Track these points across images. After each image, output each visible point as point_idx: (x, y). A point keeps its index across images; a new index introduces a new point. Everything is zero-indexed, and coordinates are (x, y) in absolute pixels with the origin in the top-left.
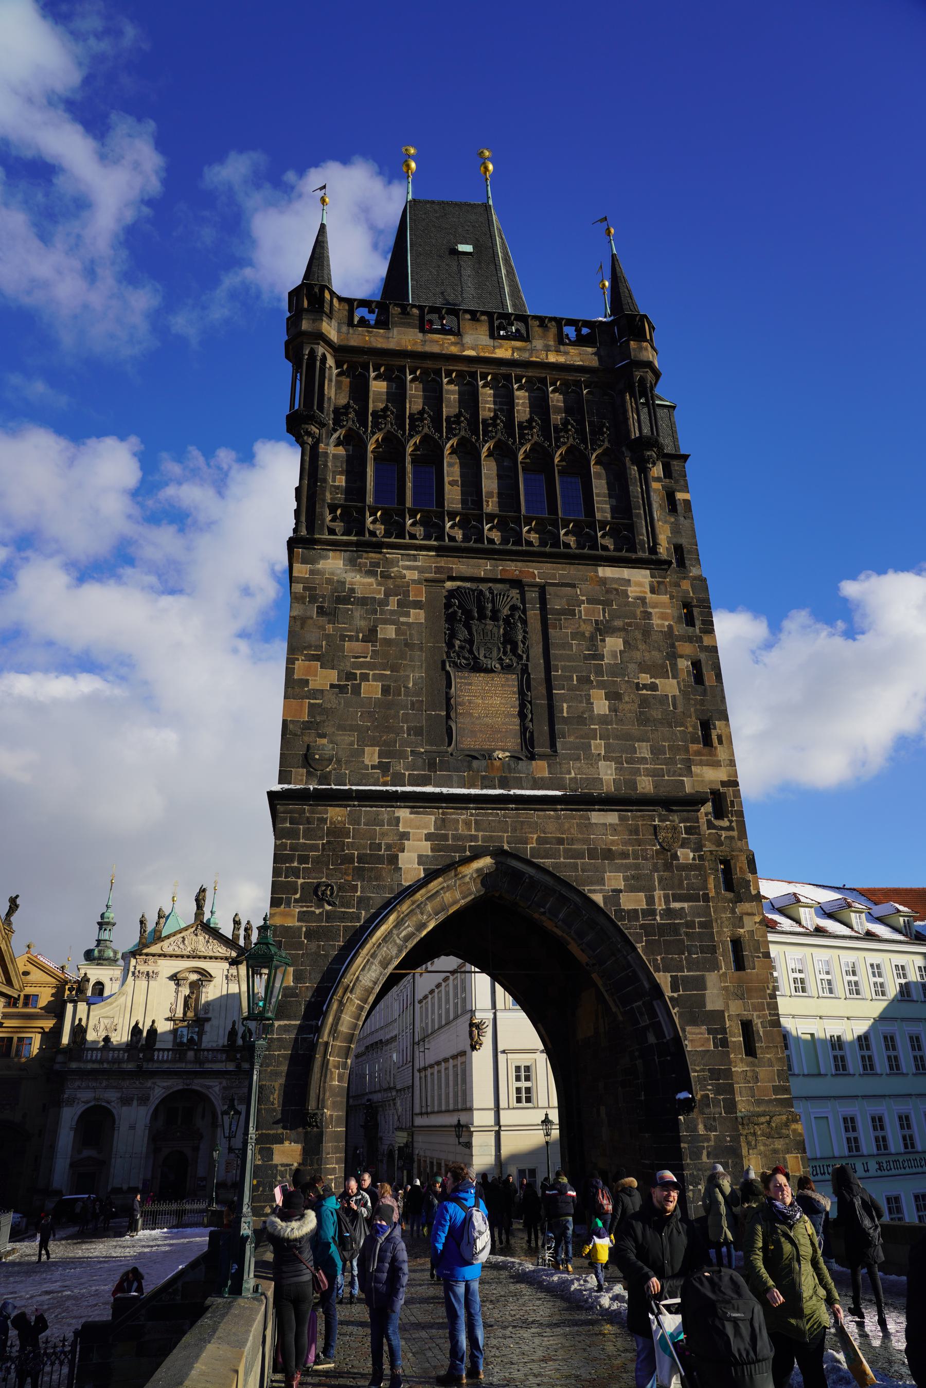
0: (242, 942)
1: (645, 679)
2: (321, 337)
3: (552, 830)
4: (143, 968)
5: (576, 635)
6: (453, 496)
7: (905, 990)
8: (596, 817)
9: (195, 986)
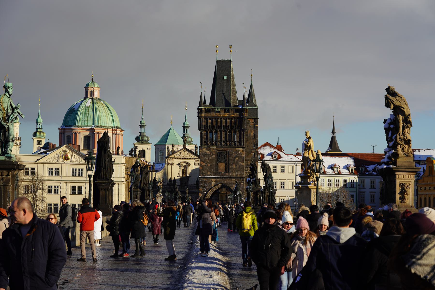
0: (198, 154)
1: (240, 163)
2: (201, 117)
3: (228, 181)
4: (169, 162)
5: (233, 158)
6: (219, 138)
7: (345, 185)
8: (233, 179)
9: (185, 167)
